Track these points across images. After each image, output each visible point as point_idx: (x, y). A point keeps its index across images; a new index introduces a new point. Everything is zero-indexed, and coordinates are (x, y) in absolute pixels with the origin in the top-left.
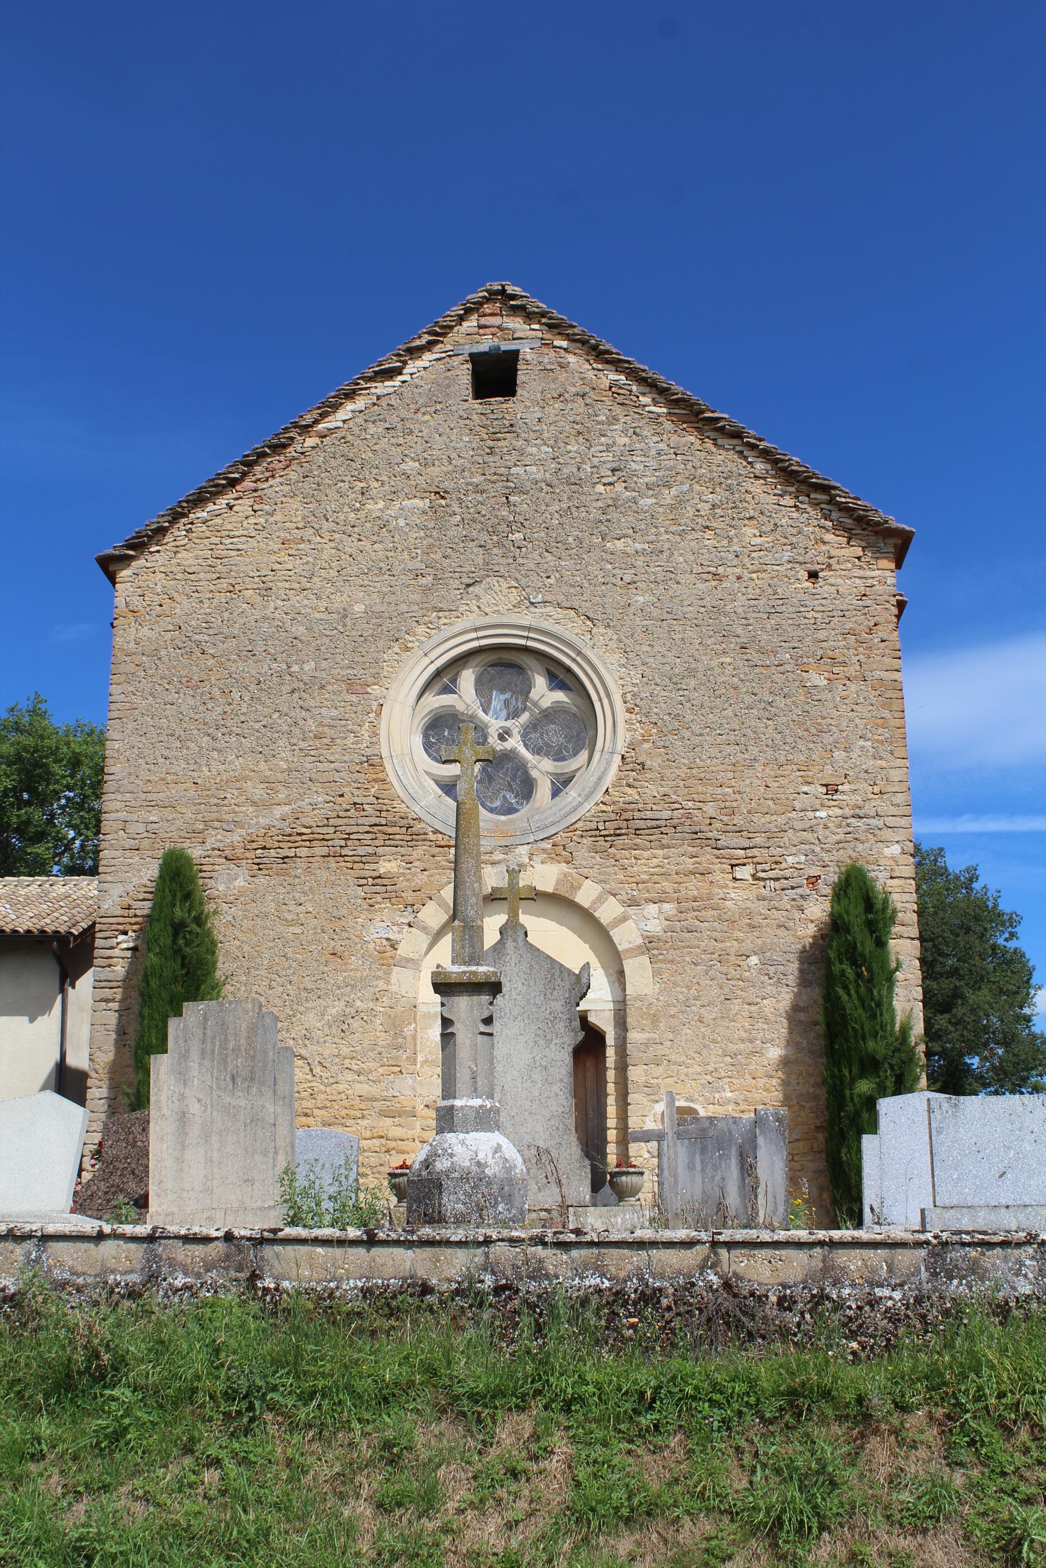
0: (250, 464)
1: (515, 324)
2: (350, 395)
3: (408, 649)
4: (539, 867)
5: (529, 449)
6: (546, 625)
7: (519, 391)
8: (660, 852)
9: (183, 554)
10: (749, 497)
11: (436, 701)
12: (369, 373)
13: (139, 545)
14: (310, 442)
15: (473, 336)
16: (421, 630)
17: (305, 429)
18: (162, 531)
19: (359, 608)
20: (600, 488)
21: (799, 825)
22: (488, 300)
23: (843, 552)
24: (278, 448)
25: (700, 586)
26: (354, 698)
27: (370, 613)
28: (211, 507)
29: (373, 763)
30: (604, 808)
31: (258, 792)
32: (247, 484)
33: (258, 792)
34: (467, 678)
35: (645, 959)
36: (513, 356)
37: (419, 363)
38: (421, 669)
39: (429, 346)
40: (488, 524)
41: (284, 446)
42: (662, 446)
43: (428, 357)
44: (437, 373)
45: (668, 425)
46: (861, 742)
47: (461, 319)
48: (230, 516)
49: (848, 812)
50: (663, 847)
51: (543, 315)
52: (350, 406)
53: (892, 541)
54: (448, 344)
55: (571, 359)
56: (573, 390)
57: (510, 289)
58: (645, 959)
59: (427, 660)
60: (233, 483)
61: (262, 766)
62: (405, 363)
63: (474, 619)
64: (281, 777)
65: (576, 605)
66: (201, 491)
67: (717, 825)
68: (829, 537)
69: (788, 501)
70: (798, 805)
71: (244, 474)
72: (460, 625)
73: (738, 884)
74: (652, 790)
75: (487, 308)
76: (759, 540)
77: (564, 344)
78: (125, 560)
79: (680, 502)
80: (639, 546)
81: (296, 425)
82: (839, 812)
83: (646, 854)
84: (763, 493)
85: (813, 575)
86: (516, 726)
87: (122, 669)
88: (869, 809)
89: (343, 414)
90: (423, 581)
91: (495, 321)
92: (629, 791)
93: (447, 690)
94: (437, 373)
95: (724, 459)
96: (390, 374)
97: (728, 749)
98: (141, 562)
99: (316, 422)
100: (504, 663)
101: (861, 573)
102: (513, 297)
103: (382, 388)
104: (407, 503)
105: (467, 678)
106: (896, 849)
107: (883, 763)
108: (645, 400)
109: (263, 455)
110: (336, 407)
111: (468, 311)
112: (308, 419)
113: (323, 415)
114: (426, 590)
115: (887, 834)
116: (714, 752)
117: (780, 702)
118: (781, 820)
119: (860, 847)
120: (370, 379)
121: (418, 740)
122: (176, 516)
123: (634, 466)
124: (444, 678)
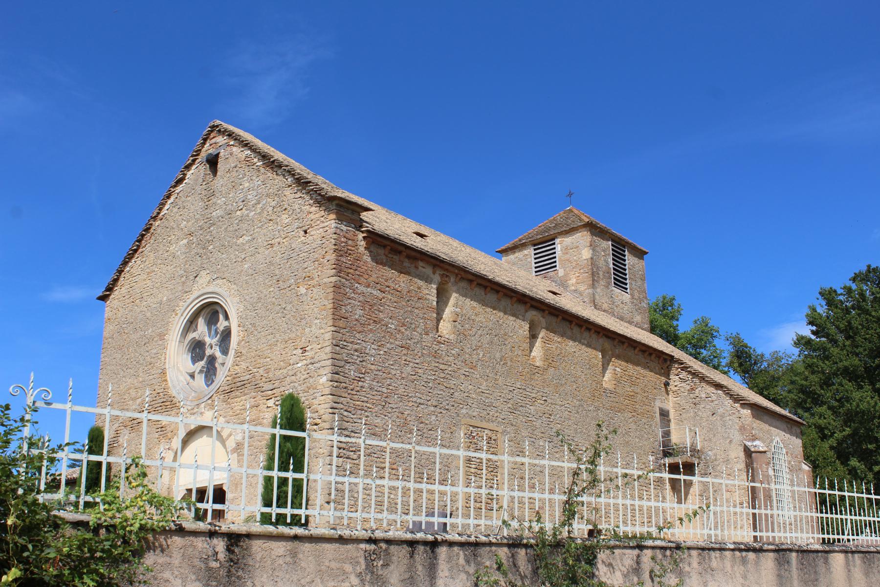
0: (140, 241)
1: (221, 140)
2: (168, 197)
3: (176, 315)
4: (207, 413)
5: (219, 202)
6: (217, 290)
7: (218, 173)
8: (243, 398)
9: (123, 289)
10: (284, 198)
11: (191, 336)
12: (173, 183)
13: (110, 289)
14: (157, 223)
15: (208, 150)
16: (181, 303)
17: (154, 218)
18: (115, 281)
19: (165, 299)
20: (239, 213)
21: (291, 373)
22: (212, 131)
23: (317, 215)
24: (147, 230)
25: (267, 252)
26: (161, 342)
27: (169, 300)
28: (130, 264)
29: (164, 373)
30: (228, 378)
31: (133, 393)
32: (140, 250)
33: (133, 393)
34: (201, 322)
35: (235, 455)
36: (217, 155)
37: (191, 172)
38: (178, 323)
39: (194, 161)
40: (203, 245)
41: (150, 228)
42: (259, 182)
43: (194, 167)
44: (197, 172)
45: (262, 170)
46: (316, 321)
47: (204, 143)
48: (135, 265)
49: (309, 361)
50: (245, 395)
51: (225, 131)
52: (169, 202)
53: (334, 203)
54: (200, 159)
55: (235, 149)
56: (233, 165)
57: (218, 122)
58: (235, 455)
59: (183, 318)
60: (136, 251)
61: (136, 381)
62: (185, 175)
63: (196, 294)
64: (140, 385)
65: (226, 275)
66: (125, 258)
67: (264, 379)
68: (313, 209)
69: (299, 195)
70: (291, 362)
71: (138, 246)
72: (192, 297)
73: (269, 410)
74: (244, 365)
75: (212, 135)
76: (287, 220)
77: (232, 143)
78: (108, 296)
79: (263, 209)
80: (247, 238)
81: (152, 218)
82: (305, 362)
83: (239, 399)
84: (291, 194)
85: (306, 232)
86: (215, 341)
87: (105, 346)
88: (316, 360)
89: (167, 207)
90: (183, 279)
91: (213, 141)
92: (236, 367)
93: (195, 331)
94: (197, 172)
95: (279, 181)
96: (180, 181)
97: (269, 337)
98: (112, 296)
99: (159, 213)
100: (211, 311)
101: (322, 225)
102: (217, 126)
103: (179, 188)
104: (182, 243)
105: (201, 322)
106: (324, 379)
107: (322, 331)
108: (256, 160)
109: (143, 236)
110: (163, 204)
111: (205, 140)
112: (155, 214)
113: (160, 209)
114: (184, 283)
115: (322, 371)
116: (264, 340)
117: (289, 307)
118: (285, 371)
119: (311, 380)
120: (175, 186)
121: (188, 358)
122: (120, 272)
123: (249, 197)
124: (191, 323)
